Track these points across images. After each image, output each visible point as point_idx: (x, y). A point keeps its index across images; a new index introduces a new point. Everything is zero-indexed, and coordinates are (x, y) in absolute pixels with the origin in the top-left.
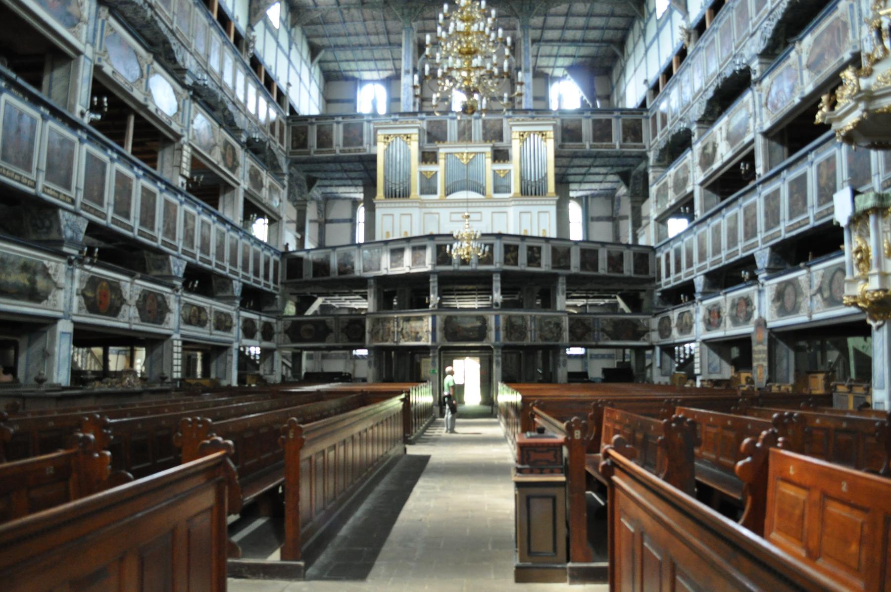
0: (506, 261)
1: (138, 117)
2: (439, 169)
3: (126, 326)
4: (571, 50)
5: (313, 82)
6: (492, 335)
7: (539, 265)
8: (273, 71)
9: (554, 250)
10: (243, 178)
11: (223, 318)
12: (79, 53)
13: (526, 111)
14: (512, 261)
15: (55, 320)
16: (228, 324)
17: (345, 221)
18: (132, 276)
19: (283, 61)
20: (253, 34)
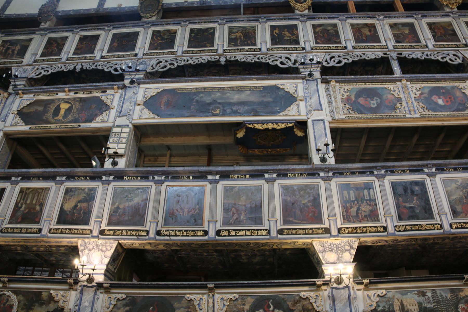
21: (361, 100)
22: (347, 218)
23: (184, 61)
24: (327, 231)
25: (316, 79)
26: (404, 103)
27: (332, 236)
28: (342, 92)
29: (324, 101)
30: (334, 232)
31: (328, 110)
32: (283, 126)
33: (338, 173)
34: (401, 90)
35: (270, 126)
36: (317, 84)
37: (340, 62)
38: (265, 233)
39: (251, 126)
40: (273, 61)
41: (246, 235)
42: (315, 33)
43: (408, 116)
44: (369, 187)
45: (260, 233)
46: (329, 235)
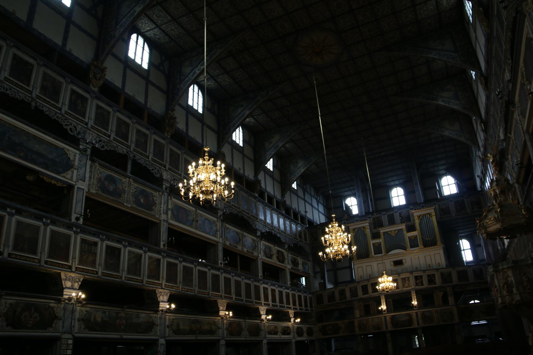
0: (417, 284)
1: (241, 255)
2: (381, 241)
3: (244, 339)
4: (443, 162)
5: (320, 205)
6: (415, 322)
7: (435, 283)
8: (297, 210)
9: (442, 274)
10: (288, 264)
11: (286, 329)
12: (218, 242)
13: (420, 204)
14: (420, 284)
15: (219, 340)
16: (289, 331)
17: (345, 268)
18: (244, 319)
19: (302, 202)
20: (285, 199)
21: (106, 183)
22: (81, 262)
23: (4, 88)
24: (70, 267)
25: (87, 155)
26: (126, 195)
27: (72, 272)
28: (98, 173)
29: (87, 175)
30: (74, 270)
31: (88, 183)
32: (60, 184)
33: (83, 231)
34: (127, 184)
35: (53, 182)
36: (87, 159)
37: (103, 147)
38: (37, 261)
39: (41, 176)
40: (66, 125)
41: (26, 260)
42: (97, 114)
43: (125, 204)
44: (96, 244)
45: (35, 260)
46: (70, 270)
